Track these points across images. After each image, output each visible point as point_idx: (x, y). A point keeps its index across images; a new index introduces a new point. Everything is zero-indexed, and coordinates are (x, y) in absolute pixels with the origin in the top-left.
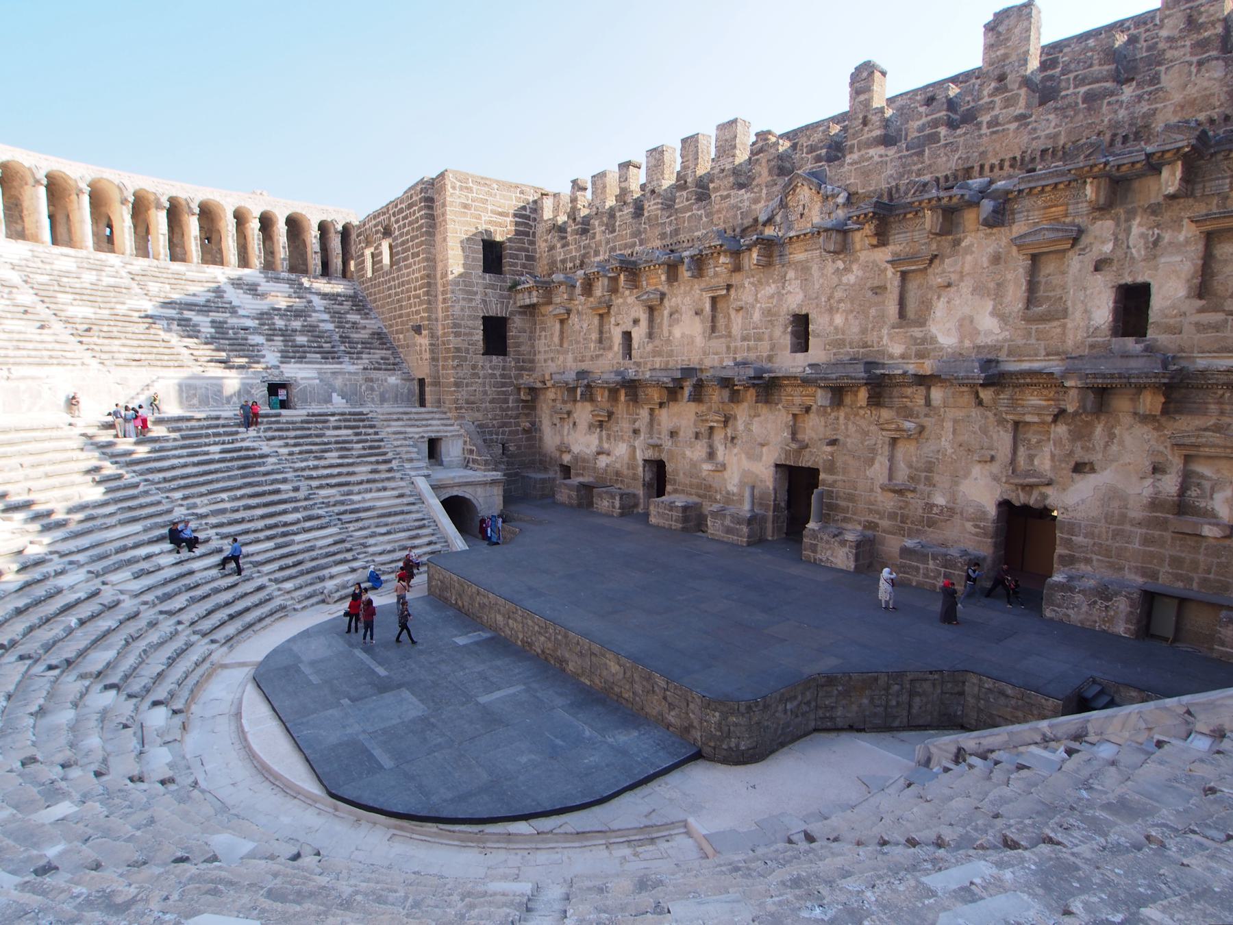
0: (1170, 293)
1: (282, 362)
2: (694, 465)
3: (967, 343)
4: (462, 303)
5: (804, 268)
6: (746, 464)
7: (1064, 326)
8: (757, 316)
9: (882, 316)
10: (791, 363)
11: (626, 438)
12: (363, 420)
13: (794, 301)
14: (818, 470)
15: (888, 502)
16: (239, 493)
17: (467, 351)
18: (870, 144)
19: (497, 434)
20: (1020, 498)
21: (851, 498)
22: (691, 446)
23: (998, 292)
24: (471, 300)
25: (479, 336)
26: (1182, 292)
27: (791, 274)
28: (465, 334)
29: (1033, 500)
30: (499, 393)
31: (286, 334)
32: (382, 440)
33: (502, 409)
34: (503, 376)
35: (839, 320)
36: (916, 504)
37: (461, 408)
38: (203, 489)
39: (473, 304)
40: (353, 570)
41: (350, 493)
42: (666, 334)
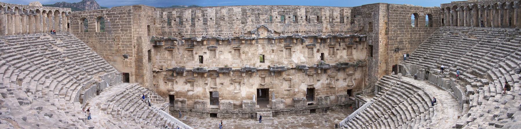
0: (326, 55)
2: (230, 91)
5: (263, 45)
6: (248, 90)
8: (250, 54)
9: (282, 57)
10: (259, 65)
11: (201, 85)
13: (260, 51)
14: (268, 89)
15: (286, 93)
18: (277, 22)
20: (309, 87)
21: (278, 93)
22: (228, 87)
23: (304, 53)
27: (260, 45)
29: (311, 87)
35: (272, 56)
36: (292, 92)
42: (217, 56)
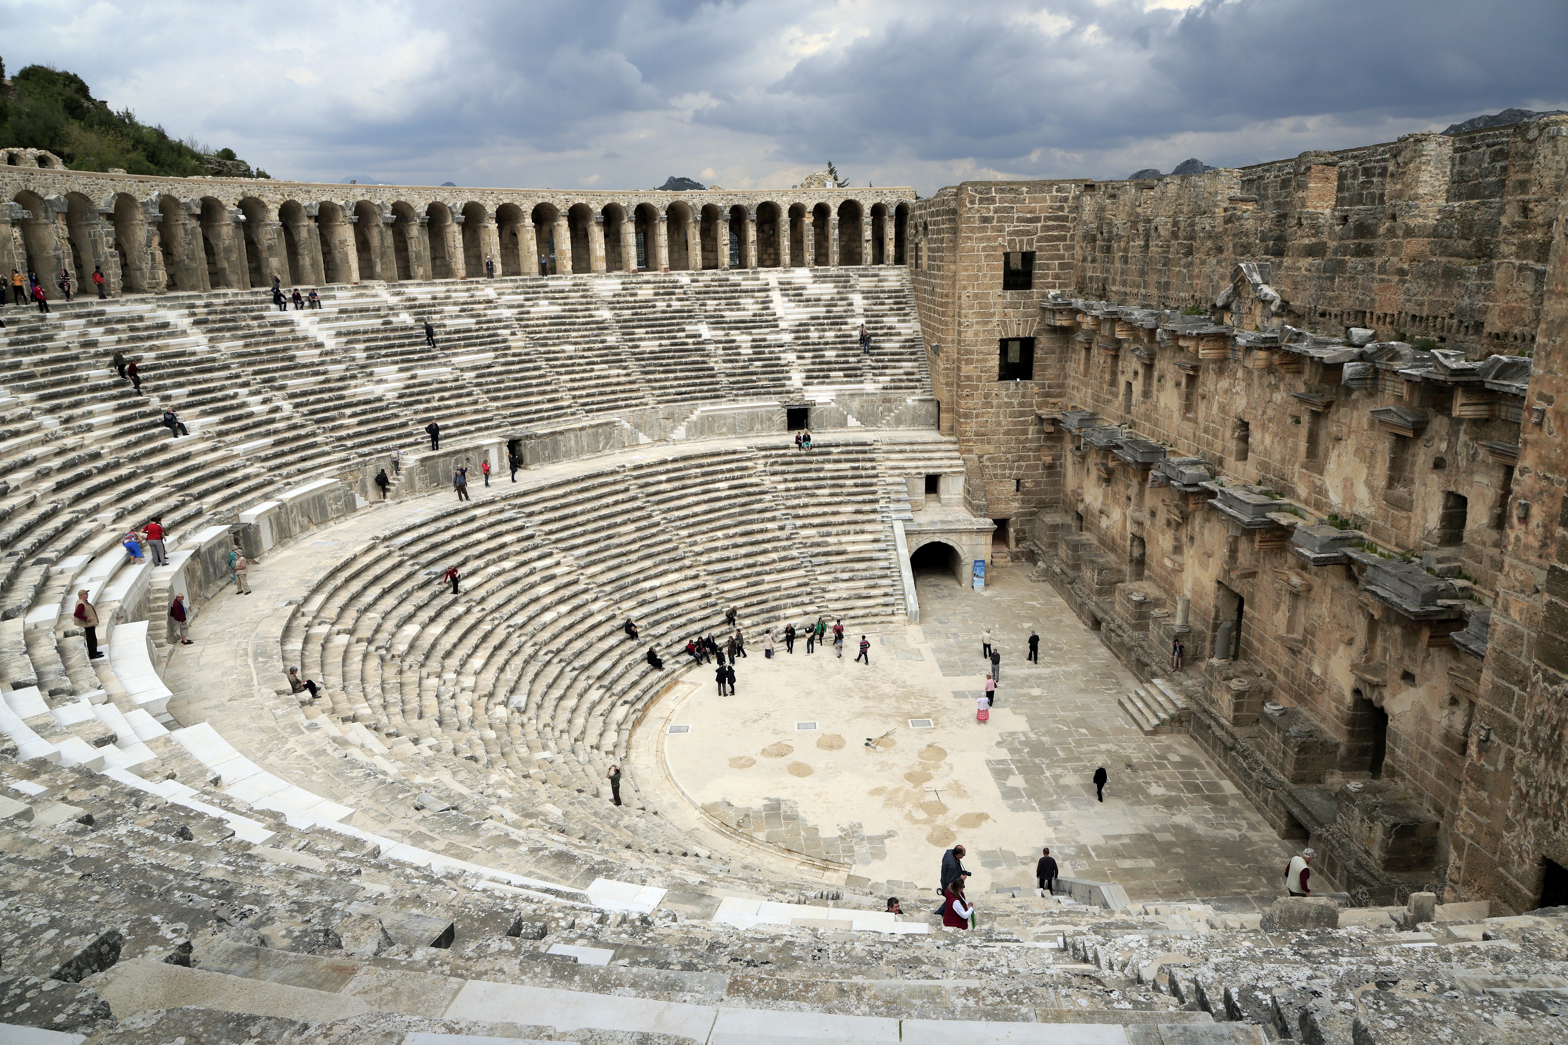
1: (805, 384)
3: (1348, 509)
4: (976, 327)
7: (1409, 519)
12: (865, 452)
16: (731, 531)
17: (979, 379)
19: (1011, 469)
24: (987, 323)
25: (994, 361)
26: (1485, 521)
28: (978, 361)
30: (1015, 424)
31: (817, 349)
32: (876, 476)
33: (1018, 441)
34: (1021, 404)
37: (968, 441)
38: (704, 528)
39: (990, 327)
40: (806, 614)
41: (829, 534)
